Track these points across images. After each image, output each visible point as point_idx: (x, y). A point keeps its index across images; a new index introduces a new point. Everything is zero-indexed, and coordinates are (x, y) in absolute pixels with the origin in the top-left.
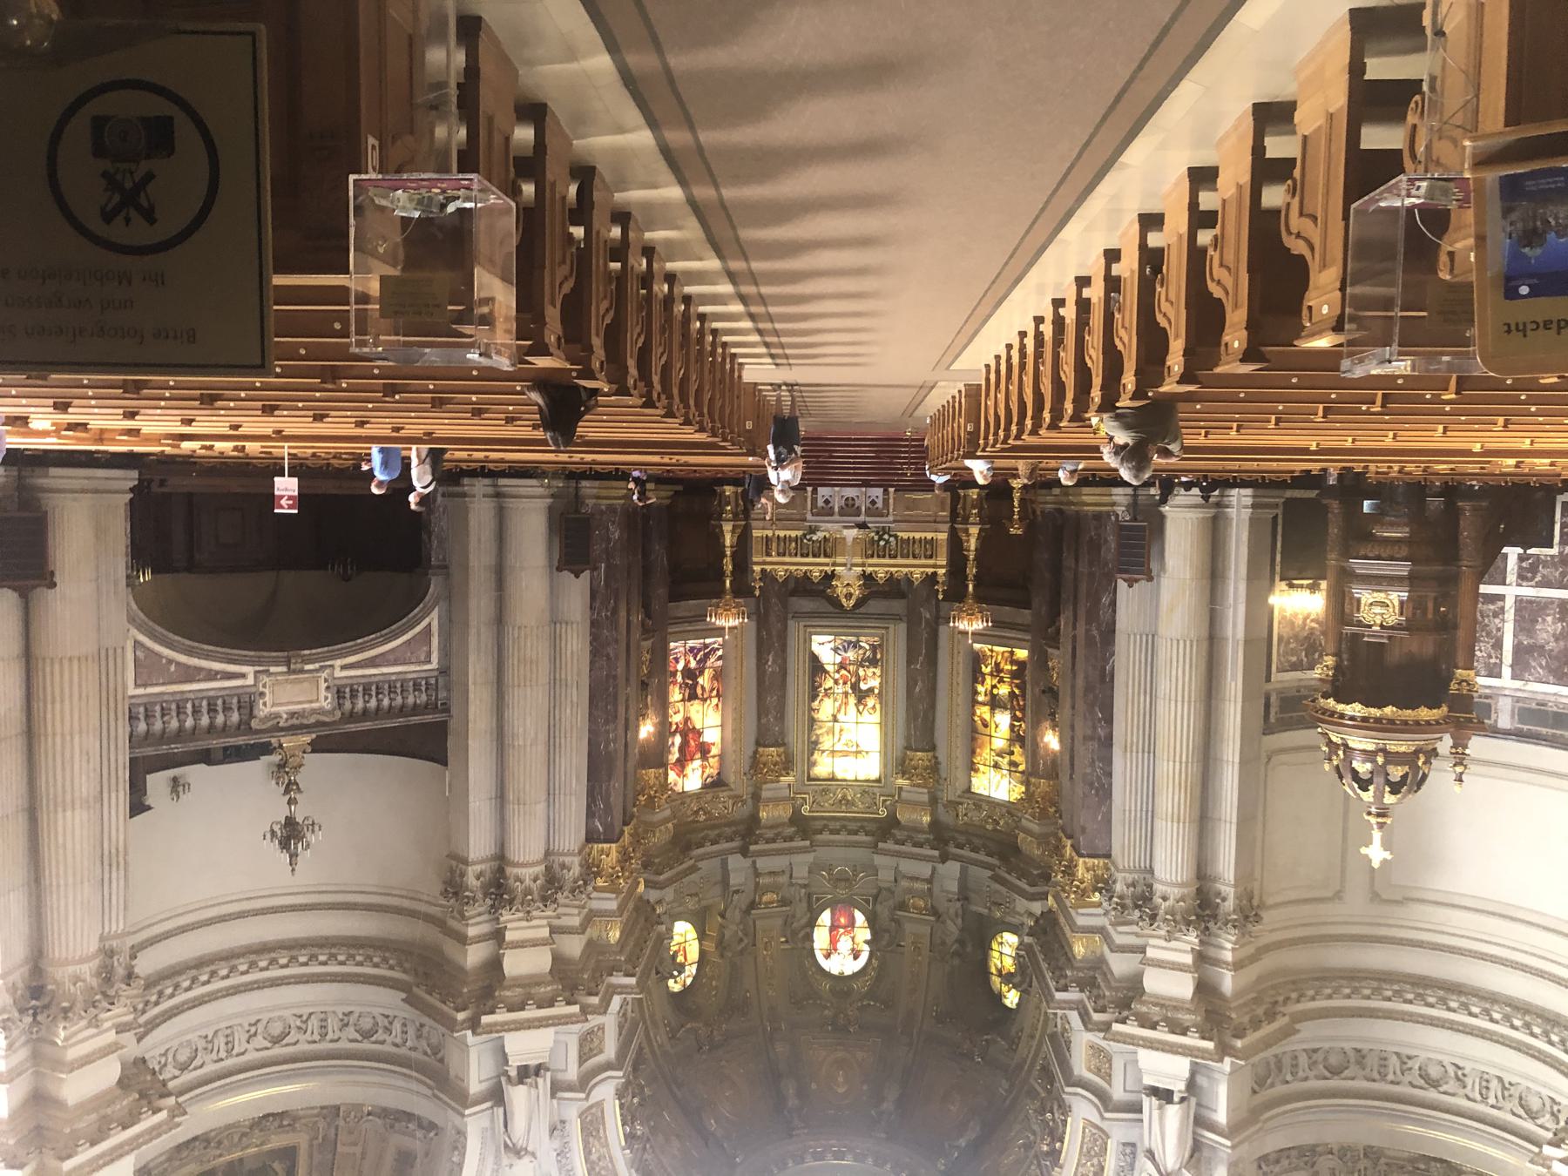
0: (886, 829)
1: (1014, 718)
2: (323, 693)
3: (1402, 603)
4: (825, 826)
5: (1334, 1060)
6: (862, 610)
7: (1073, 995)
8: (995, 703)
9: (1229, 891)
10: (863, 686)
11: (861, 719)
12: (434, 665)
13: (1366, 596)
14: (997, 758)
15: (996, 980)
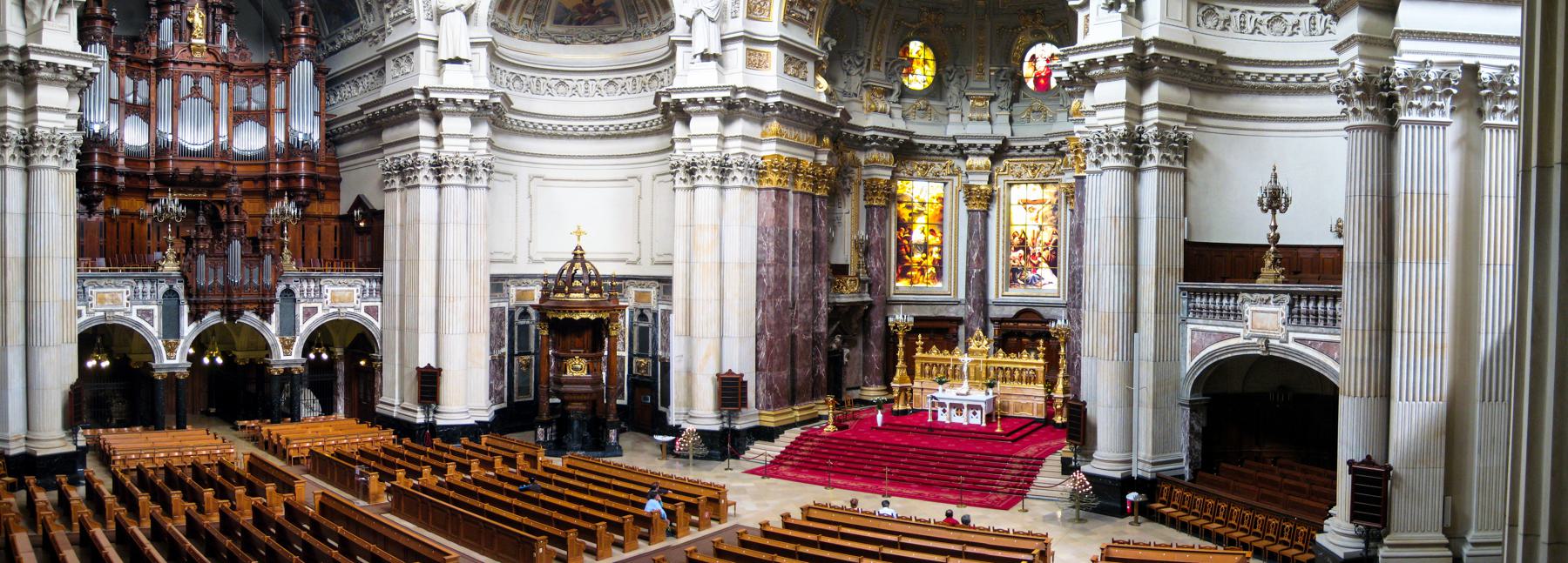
0: (1000, 152)
1: (909, 239)
2: (1249, 317)
3: (566, 372)
4: (1045, 150)
5: (655, 82)
6: (1021, 308)
7: (771, 101)
8: (925, 248)
9: (679, 184)
10: (1021, 252)
11: (1024, 228)
12: (1190, 327)
13: (584, 374)
14: (923, 209)
15: (929, 55)
